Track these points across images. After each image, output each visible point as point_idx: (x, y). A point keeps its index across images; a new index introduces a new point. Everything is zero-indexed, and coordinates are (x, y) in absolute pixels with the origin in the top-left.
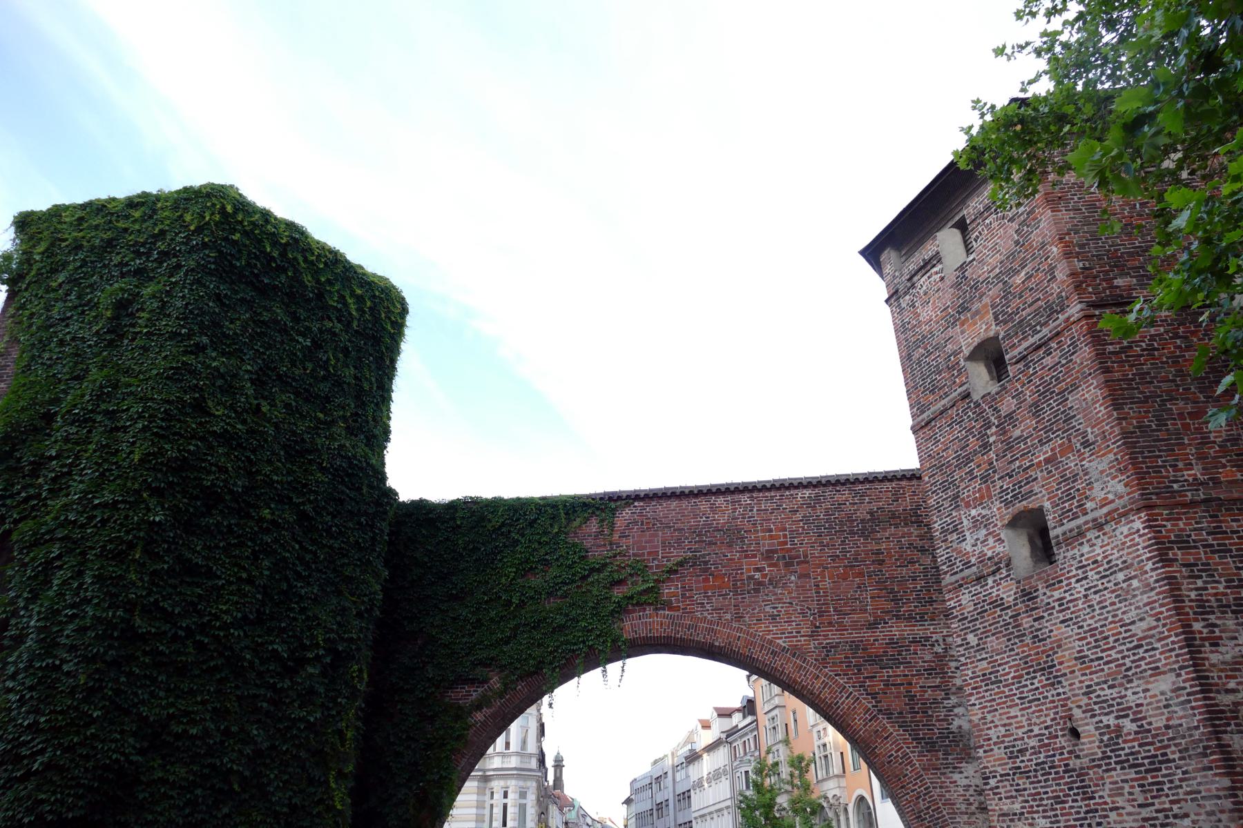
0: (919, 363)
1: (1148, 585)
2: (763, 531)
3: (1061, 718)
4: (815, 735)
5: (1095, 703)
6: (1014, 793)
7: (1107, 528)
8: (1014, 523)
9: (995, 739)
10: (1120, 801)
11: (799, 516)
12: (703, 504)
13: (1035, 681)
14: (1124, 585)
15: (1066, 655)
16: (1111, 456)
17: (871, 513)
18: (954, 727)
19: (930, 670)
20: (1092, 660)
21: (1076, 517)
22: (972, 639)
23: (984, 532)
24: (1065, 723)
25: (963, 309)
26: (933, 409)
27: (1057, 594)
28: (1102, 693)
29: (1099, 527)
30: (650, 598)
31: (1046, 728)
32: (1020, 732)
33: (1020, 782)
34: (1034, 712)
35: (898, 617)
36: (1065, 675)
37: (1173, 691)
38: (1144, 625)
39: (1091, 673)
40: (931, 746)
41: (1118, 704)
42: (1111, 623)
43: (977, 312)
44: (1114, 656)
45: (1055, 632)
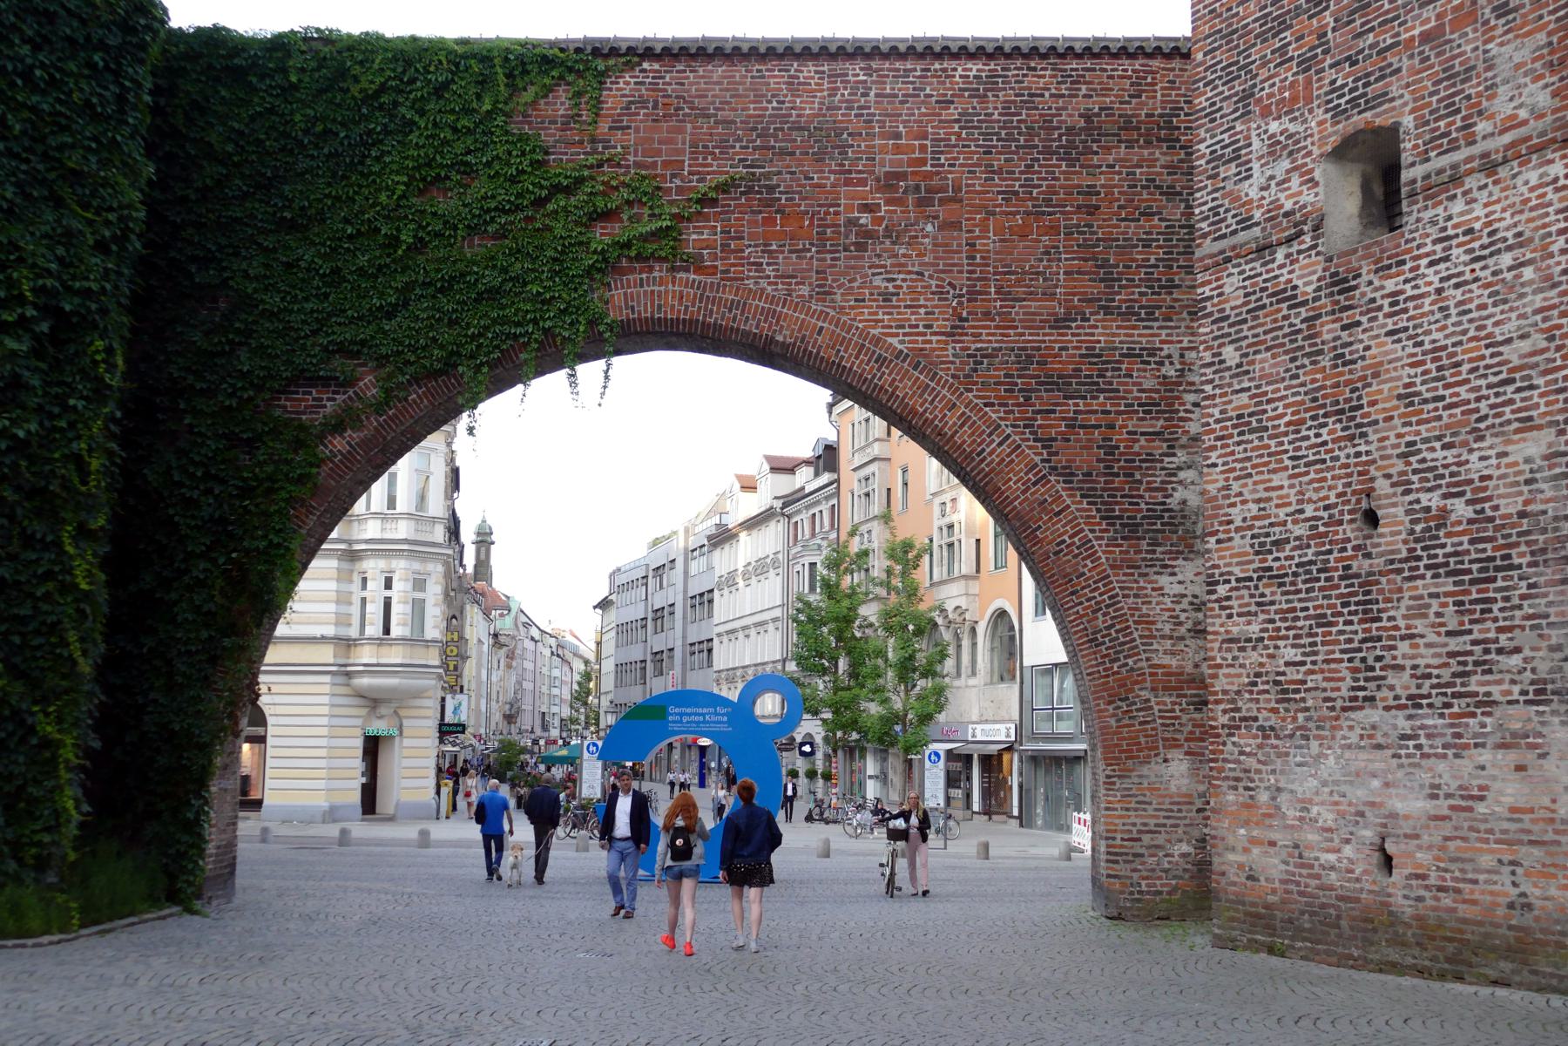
1: (1549, 277)
2: (883, 136)
3: (1354, 493)
4: (937, 510)
5: (1415, 472)
6: (1253, 608)
7: (1503, 172)
8: (1340, 153)
9: (1238, 523)
10: (1420, 626)
11: (953, 112)
12: (775, 76)
13: (1324, 431)
14: (1509, 276)
16: (1542, 38)
17: (1087, 117)
18: (1173, 502)
19: (1149, 407)
20: (1426, 401)
21: (1453, 147)
22: (1230, 354)
23: (1286, 164)
24: (1359, 501)
27: (1390, 285)
28: (1429, 456)
29: (1489, 166)
30: (662, 249)
31: (1326, 508)
32: (1282, 512)
33: (1267, 591)
34: (1311, 482)
35: (1108, 311)
36: (1376, 422)
37: (1546, 458)
38: (1524, 346)
39: (1419, 423)
40: (1132, 530)
41: (1452, 475)
42: (1471, 339)
44: (1465, 396)
45: (1373, 351)
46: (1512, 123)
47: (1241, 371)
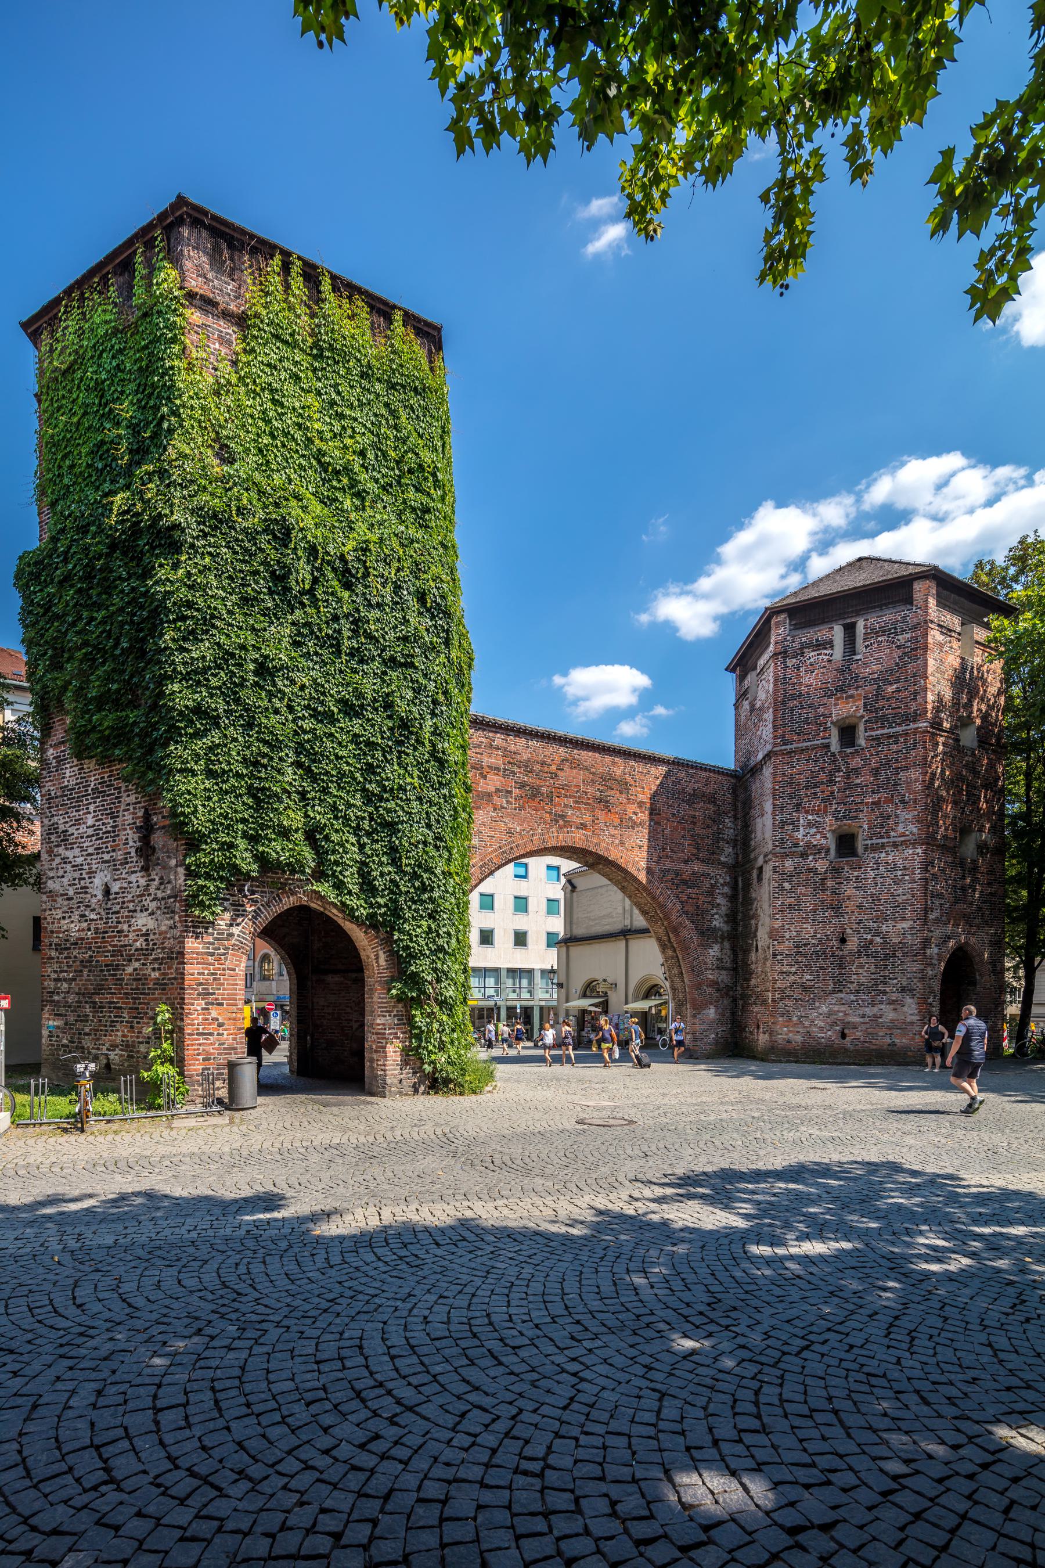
0: (792, 710)
15: (851, 905)
21: (882, 837)
25: (841, 689)
26: (795, 745)
29: (895, 845)
43: (852, 696)
46: (902, 835)
47: (791, 891)
